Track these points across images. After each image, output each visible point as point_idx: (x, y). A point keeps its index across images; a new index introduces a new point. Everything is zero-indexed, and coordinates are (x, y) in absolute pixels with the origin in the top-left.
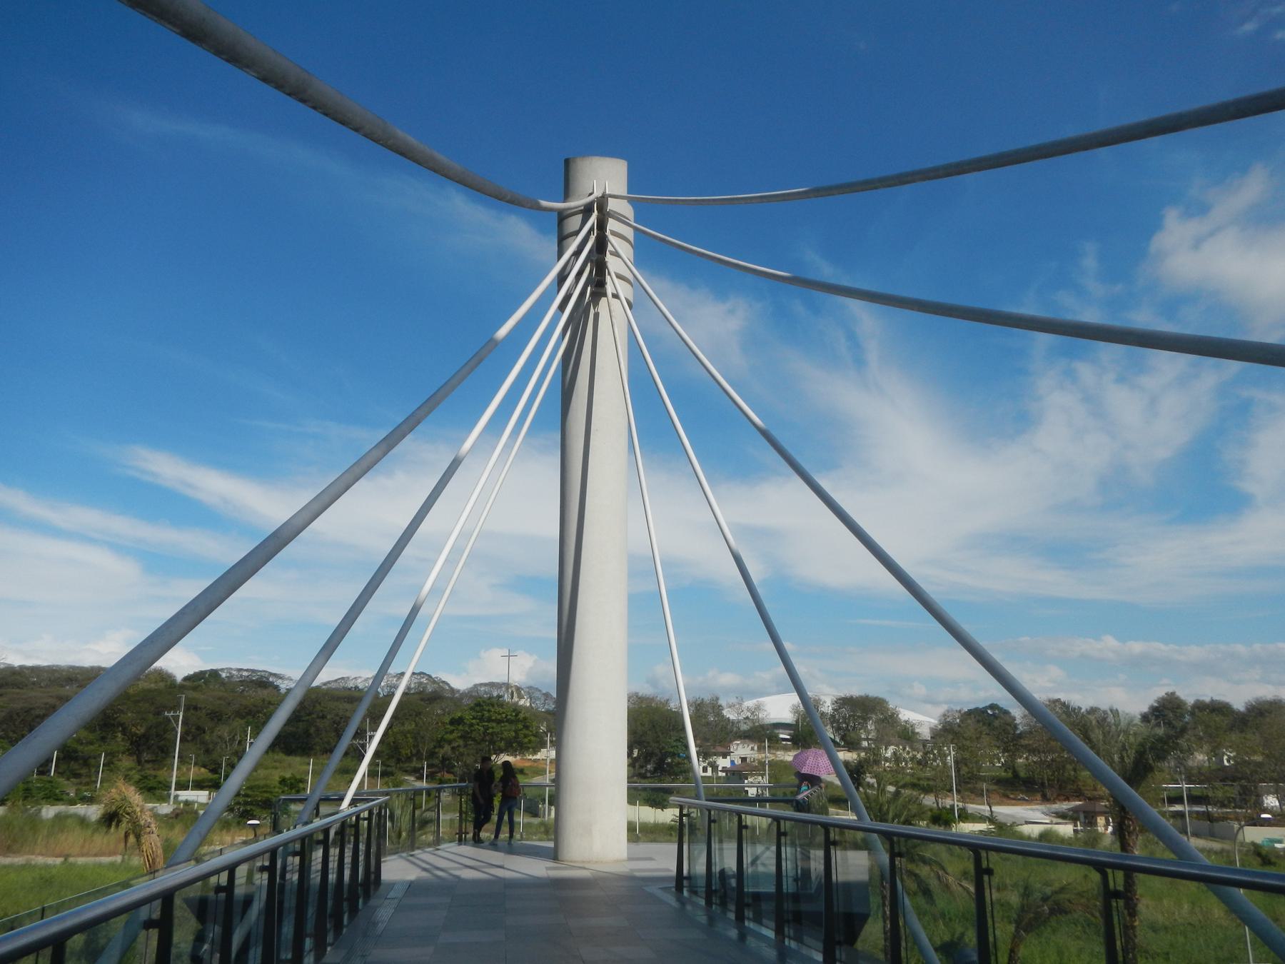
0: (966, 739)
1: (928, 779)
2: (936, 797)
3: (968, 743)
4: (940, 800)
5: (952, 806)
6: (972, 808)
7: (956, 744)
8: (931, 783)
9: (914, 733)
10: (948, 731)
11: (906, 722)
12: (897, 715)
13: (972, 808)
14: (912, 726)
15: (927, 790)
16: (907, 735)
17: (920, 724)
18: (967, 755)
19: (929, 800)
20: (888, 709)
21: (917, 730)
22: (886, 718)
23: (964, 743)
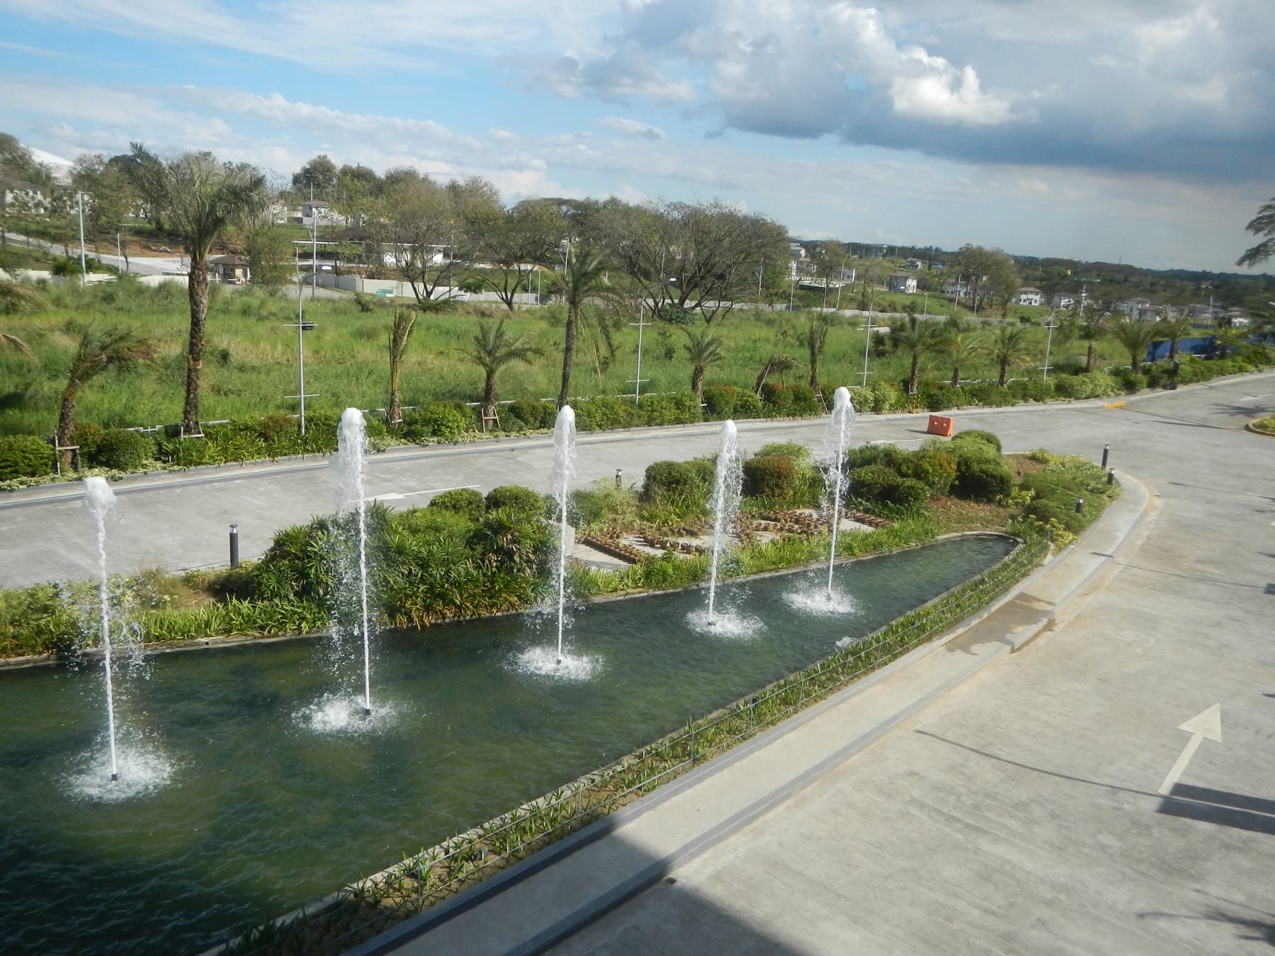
0: (105, 187)
1: (57, 227)
2: (66, 246)
3: (108, 192)
4: (70, 249)
5: (80, 256)
6: (107, 258)
7: (94, 191)
8: (61, 231)
9: (49, 177)
10: (86, 178)
11: (41, 164)
12: (30, 157)
13: (107, 258)
14: (48, 170)
15: (55, 239)
16: (40, 178)
17: (58, 167)
18: (106, 204)
19: (57, 250)
20: (18, 149)
21: (54, 175)
22: (14, 158)
23: (103, 190)
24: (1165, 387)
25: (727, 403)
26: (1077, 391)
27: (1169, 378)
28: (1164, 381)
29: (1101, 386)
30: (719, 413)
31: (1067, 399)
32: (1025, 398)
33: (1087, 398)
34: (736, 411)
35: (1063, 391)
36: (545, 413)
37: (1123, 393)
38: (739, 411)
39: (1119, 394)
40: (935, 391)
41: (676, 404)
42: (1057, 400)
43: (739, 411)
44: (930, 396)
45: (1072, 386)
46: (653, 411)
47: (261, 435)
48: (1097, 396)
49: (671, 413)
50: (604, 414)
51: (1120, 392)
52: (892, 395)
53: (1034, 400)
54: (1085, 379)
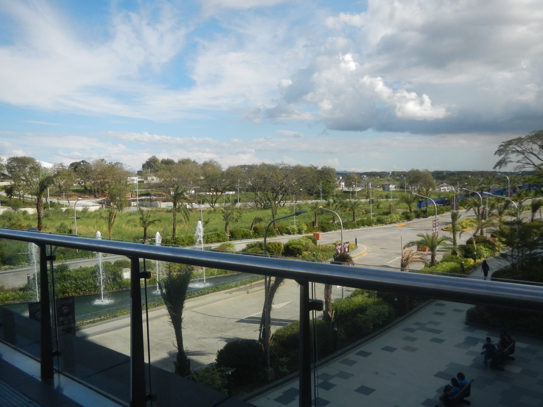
24: (424, 217)
25: (238, 234)
26: (385, 221)
27: (424, 214)
28: (422, 215)
29: (394, 219)
30: (235, 238)
31: (382, 224)
32: (363, 225)
33: (390, 223)
34: (242, 236)
35: (380, 222)
36: (166, 241)
37: (405, 221)
38: (244, 237)
39: (404, 221)
40: (323, 225)
41: (218, 235)
42: (378, 225)
43: (244, 237)
44: (322, 227)
45: (382, 220)
46: (208, 238)
47: (62, 253)
48: (395, 223)
49: (216, 238)
50: (189, 240)
51: (404, 220)
52: (305, 228)
53: (368, 226)
54: (388, 217)
